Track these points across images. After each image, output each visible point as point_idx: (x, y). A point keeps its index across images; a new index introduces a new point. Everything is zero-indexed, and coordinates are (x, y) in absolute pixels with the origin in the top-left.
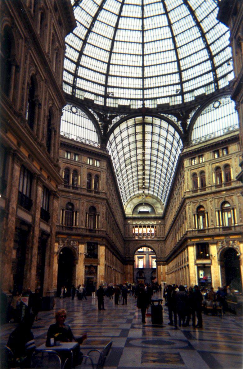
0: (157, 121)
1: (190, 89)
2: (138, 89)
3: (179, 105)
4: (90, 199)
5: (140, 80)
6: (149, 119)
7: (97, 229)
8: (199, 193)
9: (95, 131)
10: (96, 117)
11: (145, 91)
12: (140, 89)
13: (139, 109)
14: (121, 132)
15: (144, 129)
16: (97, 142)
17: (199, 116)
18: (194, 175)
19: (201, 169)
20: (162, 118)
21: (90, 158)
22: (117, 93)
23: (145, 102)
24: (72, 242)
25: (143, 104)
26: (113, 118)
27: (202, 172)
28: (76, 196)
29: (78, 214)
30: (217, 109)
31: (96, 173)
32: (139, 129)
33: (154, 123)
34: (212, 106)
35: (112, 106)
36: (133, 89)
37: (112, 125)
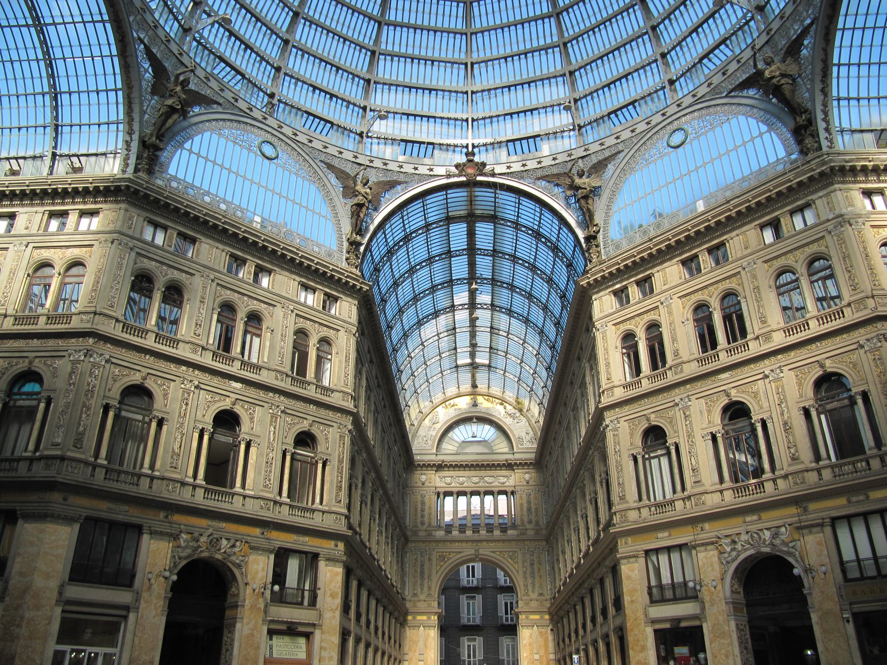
4: (300, 405)
6: (484, 197)
7: (320, 507)
8: (646, 385)
13: (457, 166)
15: (471, 234)
16: (334, 247)
24: (224, 542)
28: (252, 392)
29: (253, 450)
30: (681, 149)
32: (458, 234)
33: (497, 214)
34: (665, 144)
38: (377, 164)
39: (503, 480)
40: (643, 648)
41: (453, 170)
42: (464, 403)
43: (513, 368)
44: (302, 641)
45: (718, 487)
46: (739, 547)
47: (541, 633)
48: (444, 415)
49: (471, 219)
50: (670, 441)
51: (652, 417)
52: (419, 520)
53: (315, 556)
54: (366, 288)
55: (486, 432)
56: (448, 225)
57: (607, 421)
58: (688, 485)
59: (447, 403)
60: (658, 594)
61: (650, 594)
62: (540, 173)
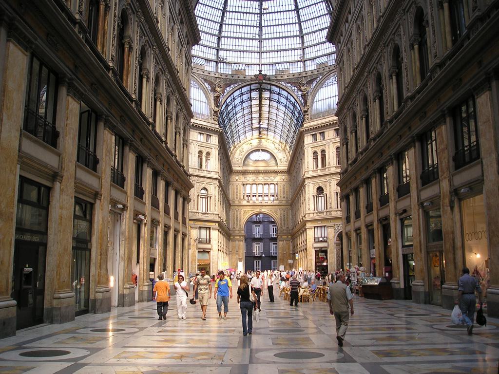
0: (274, 88)
1: (313, 55)
7: (210, 213)
8: (319, 173)
9: (207, 102)
10: (207, 86)
13: (255, 76)
18: (315, 153)
19: (322, 148)
21: (200, 133)
22: (230, 57)
25: (260, 71)
27: (323, 151)
31: (208, 150)
32: (255, 94)
34: (334, 80)
35: (225, 72)
38: (223, 77)
39: (272, 178)
40: (311, 255)
41: (253, 77)
42: (255, 143)
43: (278, 131)
44: (207, 254)
45: (337, 209)
46: (339, 228)
47: (287, 243)
48: (246, 148)
49: (260, 91)
50: (324, 193)
51: (320, 184)
52: (235, 196)
53: (210, 228)
54: (221, 131)
55: (266, 156)
56: (251, 92)
57: (306, 183)
58: (328, 208)
59: (247, 143)
60: (316, 240)
61: (315, 240)
62: (288, 81)
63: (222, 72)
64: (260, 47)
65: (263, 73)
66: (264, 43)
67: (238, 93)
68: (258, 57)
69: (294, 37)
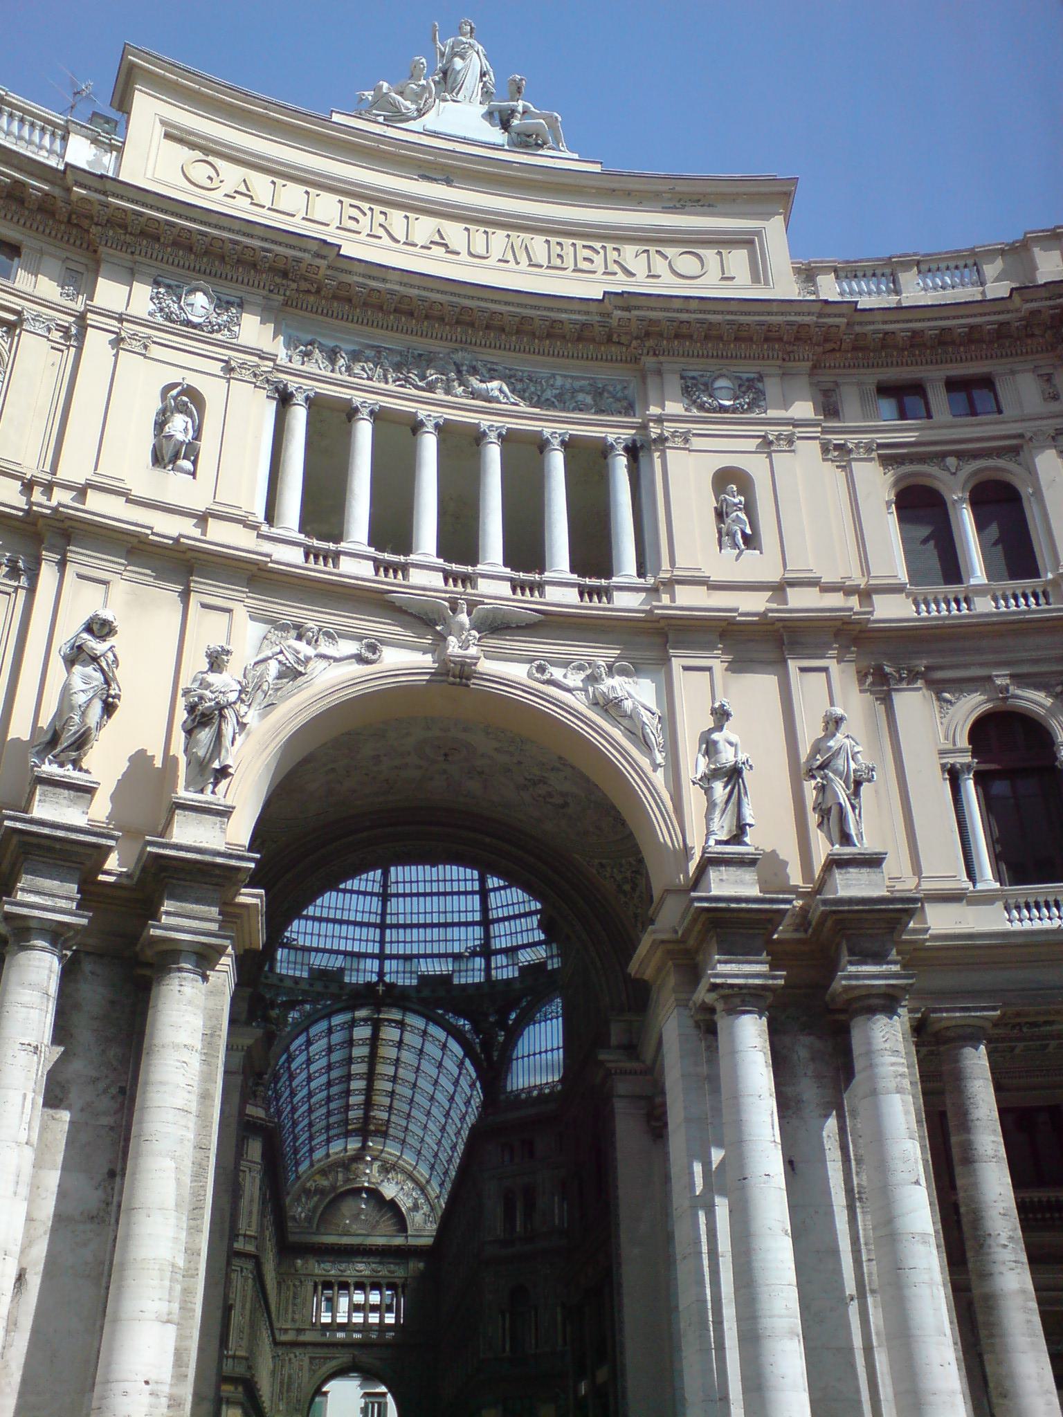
2: (368, 925)
3: (477, 986)
5: (375, 899)
11: (388, 931)
12: (375, 925)
13: (369, 986)
14: (309, 1043)
17: (528, 1025)
20: (429, 1018)
23: (387, 962)
25: (381, 974)
26: (294, 1009)
32: (362, 1032)
35: (291, 973)
36: (355, 923)
37: (289, 1029)
38: (288, 983)
49: (376, 1025)
63: (284, 972)
64: (384, 914)
65: (387, 979)
66: (393, 905)
67: (323, 1025)
68: (377, 938)
69: (466, 893)
